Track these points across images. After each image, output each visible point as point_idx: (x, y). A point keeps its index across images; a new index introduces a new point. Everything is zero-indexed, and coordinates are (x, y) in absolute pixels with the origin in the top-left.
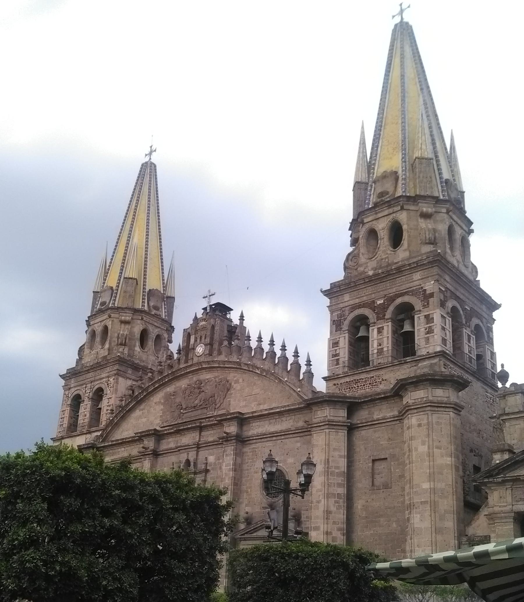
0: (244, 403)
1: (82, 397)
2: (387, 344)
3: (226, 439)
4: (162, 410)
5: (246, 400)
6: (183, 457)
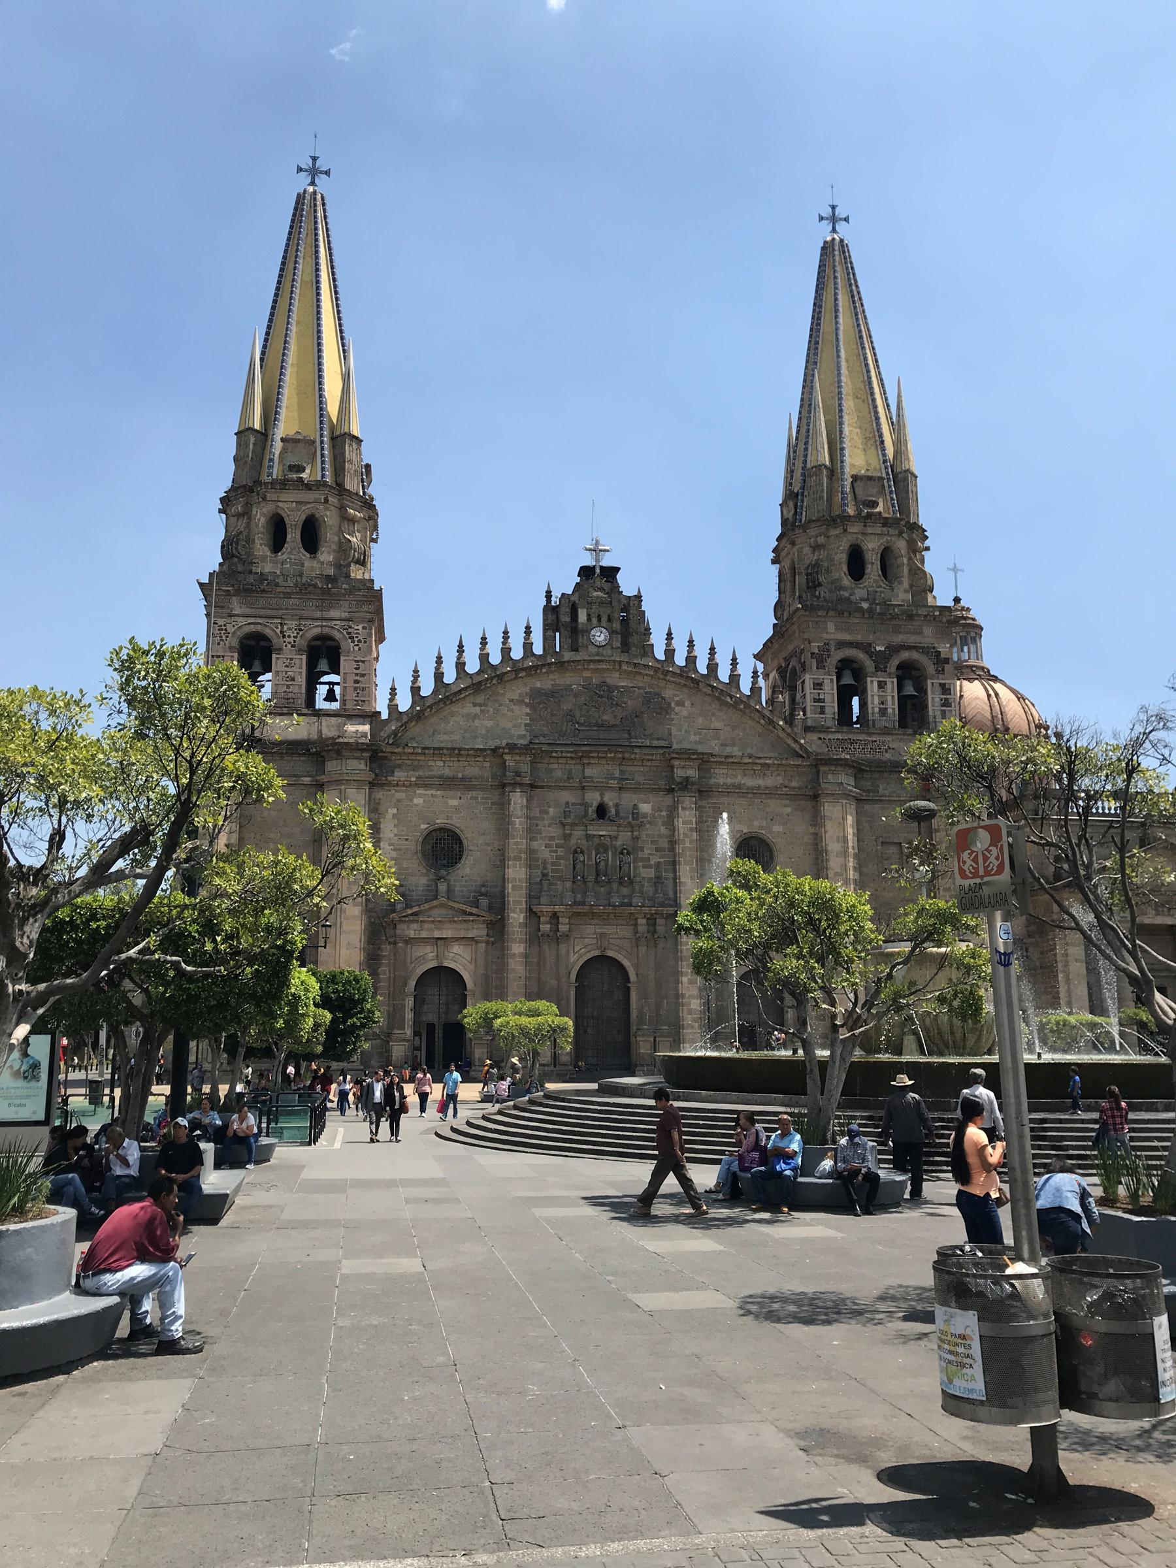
0: (697, 738)
1: (275, 641)
2: (892, 707)
3: (685, 784)
4: (527, 714)
5: (700, 734)
6: (593, 798)
